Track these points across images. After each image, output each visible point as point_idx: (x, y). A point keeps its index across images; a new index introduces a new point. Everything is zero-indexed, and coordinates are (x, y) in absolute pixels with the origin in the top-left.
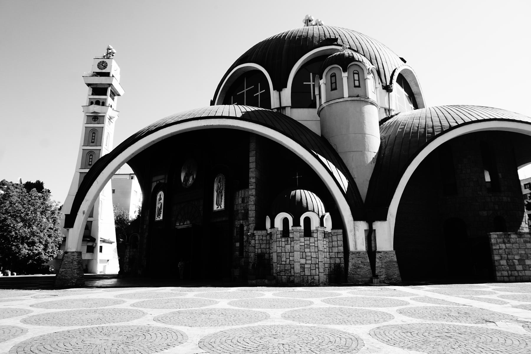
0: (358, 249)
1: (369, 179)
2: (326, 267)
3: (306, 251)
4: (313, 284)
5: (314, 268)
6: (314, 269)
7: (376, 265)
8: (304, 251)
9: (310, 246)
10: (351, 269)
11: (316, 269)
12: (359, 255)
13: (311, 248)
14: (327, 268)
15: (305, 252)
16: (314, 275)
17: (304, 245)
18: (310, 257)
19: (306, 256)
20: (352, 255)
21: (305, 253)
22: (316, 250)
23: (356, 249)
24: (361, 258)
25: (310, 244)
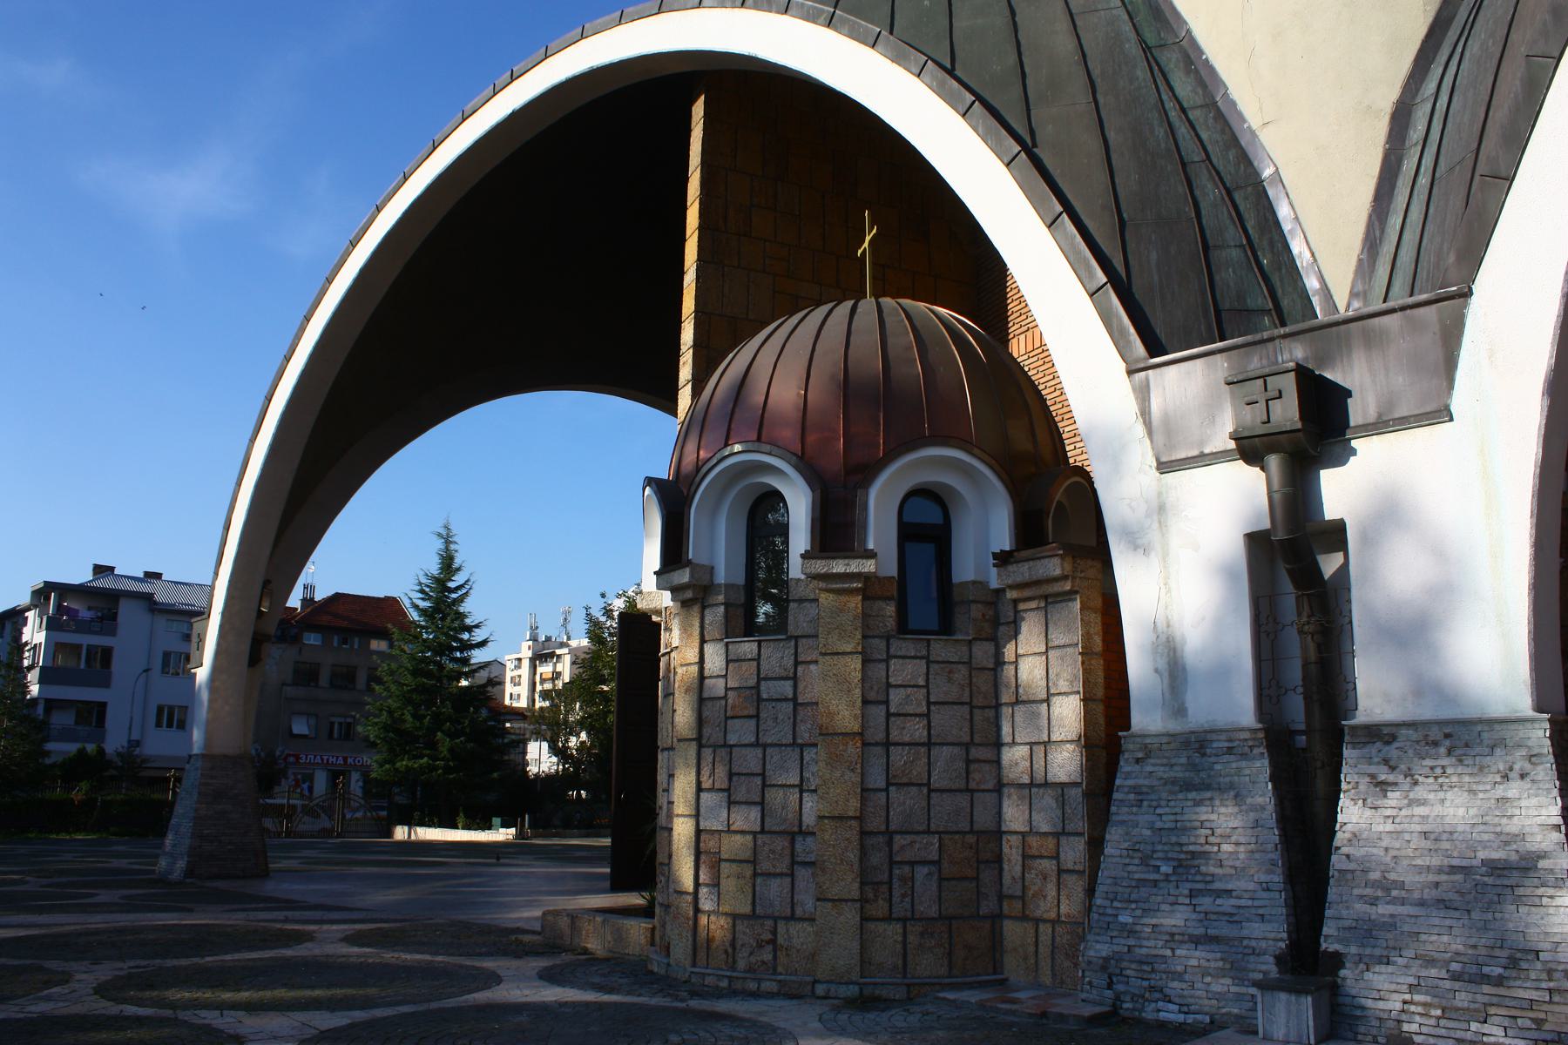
0: (1190, 712)
1: (1394, 94)
2: (912, 864)
3: (732, 739)
4: (759, 981)
5: (783, 867)
6: (781, 875)
7: (1334, 858)
8: (717, 737)
9: (759, 699)
10: (1116, 881)
11: (792, 875)
12: (1193, 767)
13: (763, 715)
14: (921, 872)
15: (725, 745)
16: (775, 919)
17: (725, 697)
18: (758, 781)
19: (731, 775)
20: (1138, 761)
21: (723, 752)
22: (802, 728)
23: (1180, 711)
24: (1208, 794)
25: (757, 687)
